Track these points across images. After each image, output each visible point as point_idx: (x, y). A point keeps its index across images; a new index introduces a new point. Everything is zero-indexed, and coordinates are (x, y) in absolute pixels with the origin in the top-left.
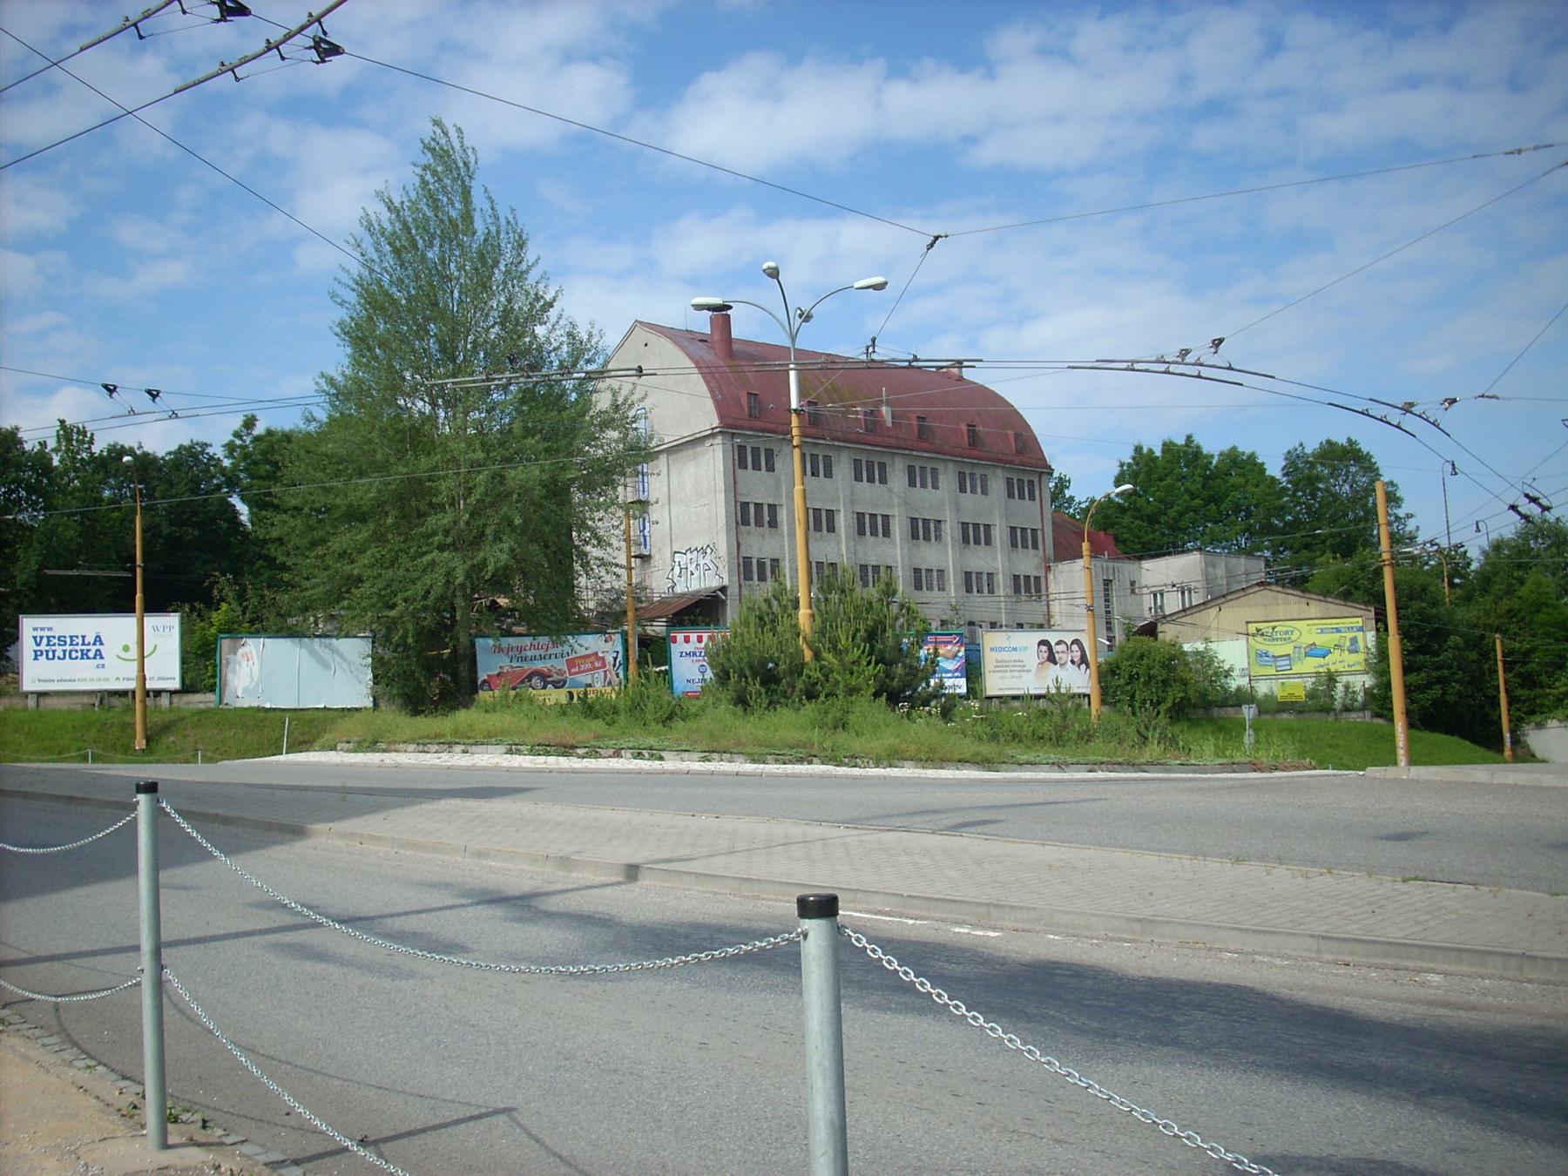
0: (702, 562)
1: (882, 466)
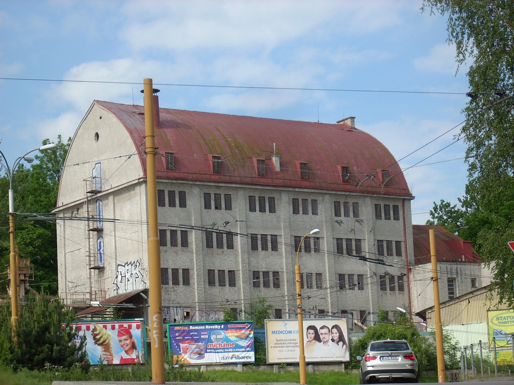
0: (134, 272)
1: (272, 200)
